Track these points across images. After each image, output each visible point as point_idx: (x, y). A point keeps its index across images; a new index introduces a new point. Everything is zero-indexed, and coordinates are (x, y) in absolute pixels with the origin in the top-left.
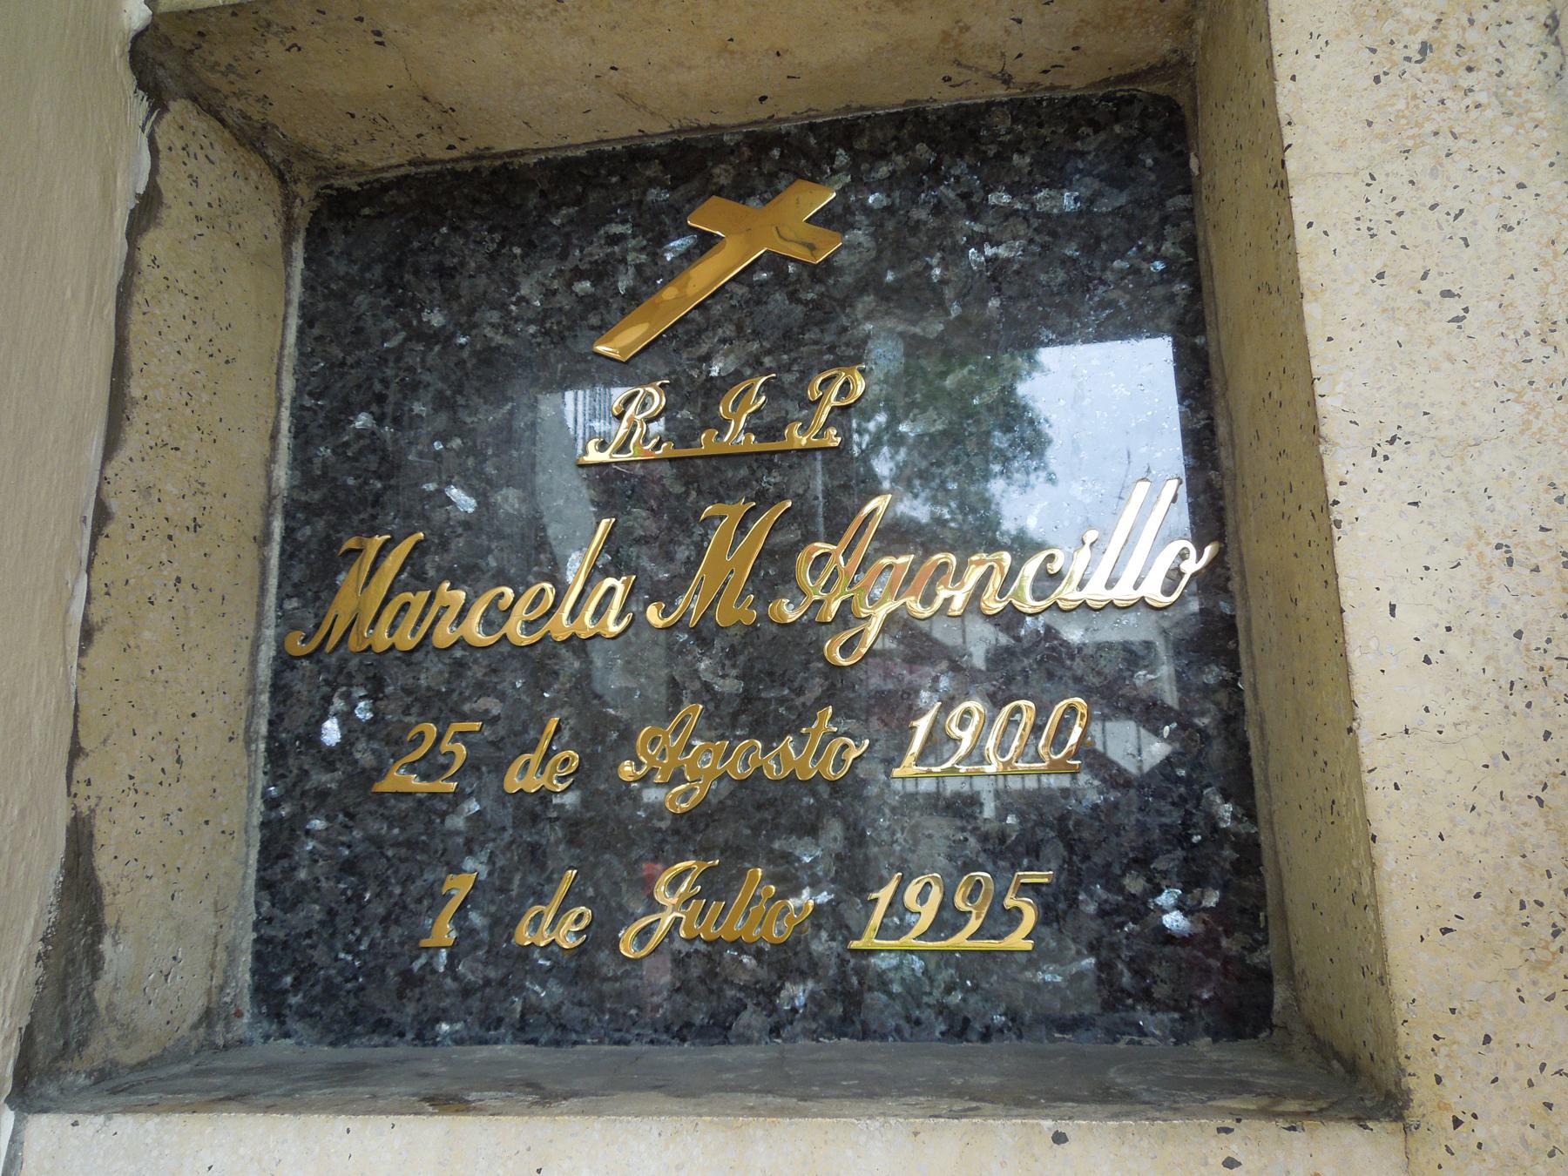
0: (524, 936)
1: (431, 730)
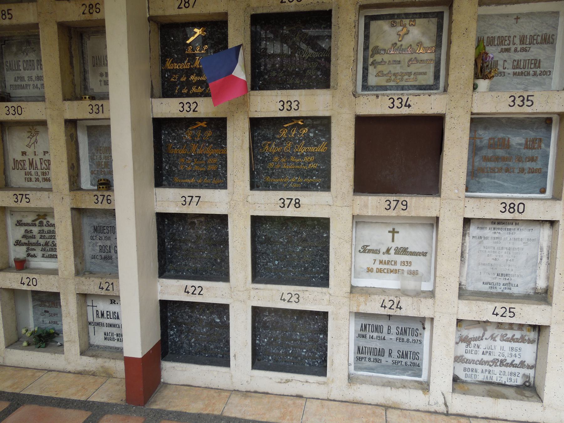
0: (183, 92)
1: (174, 75)
